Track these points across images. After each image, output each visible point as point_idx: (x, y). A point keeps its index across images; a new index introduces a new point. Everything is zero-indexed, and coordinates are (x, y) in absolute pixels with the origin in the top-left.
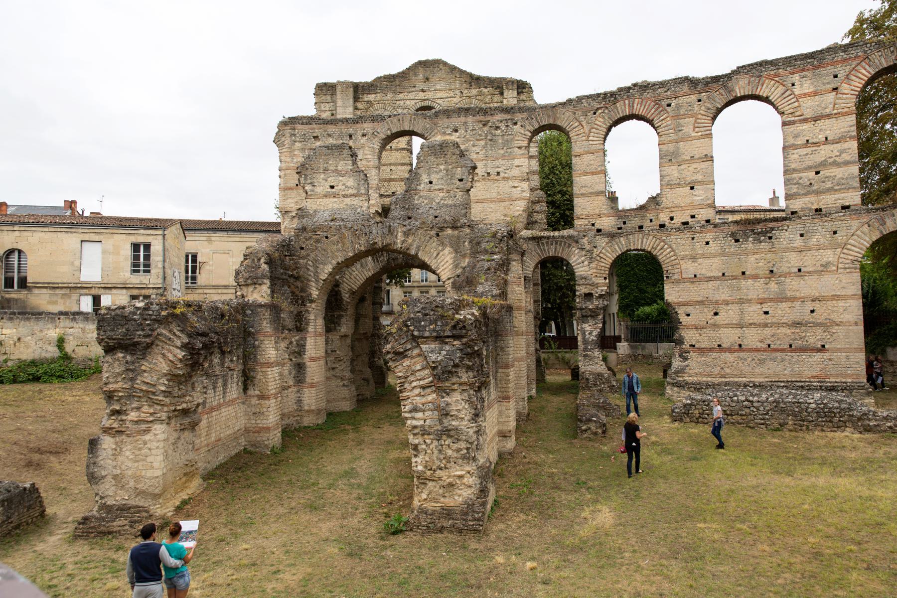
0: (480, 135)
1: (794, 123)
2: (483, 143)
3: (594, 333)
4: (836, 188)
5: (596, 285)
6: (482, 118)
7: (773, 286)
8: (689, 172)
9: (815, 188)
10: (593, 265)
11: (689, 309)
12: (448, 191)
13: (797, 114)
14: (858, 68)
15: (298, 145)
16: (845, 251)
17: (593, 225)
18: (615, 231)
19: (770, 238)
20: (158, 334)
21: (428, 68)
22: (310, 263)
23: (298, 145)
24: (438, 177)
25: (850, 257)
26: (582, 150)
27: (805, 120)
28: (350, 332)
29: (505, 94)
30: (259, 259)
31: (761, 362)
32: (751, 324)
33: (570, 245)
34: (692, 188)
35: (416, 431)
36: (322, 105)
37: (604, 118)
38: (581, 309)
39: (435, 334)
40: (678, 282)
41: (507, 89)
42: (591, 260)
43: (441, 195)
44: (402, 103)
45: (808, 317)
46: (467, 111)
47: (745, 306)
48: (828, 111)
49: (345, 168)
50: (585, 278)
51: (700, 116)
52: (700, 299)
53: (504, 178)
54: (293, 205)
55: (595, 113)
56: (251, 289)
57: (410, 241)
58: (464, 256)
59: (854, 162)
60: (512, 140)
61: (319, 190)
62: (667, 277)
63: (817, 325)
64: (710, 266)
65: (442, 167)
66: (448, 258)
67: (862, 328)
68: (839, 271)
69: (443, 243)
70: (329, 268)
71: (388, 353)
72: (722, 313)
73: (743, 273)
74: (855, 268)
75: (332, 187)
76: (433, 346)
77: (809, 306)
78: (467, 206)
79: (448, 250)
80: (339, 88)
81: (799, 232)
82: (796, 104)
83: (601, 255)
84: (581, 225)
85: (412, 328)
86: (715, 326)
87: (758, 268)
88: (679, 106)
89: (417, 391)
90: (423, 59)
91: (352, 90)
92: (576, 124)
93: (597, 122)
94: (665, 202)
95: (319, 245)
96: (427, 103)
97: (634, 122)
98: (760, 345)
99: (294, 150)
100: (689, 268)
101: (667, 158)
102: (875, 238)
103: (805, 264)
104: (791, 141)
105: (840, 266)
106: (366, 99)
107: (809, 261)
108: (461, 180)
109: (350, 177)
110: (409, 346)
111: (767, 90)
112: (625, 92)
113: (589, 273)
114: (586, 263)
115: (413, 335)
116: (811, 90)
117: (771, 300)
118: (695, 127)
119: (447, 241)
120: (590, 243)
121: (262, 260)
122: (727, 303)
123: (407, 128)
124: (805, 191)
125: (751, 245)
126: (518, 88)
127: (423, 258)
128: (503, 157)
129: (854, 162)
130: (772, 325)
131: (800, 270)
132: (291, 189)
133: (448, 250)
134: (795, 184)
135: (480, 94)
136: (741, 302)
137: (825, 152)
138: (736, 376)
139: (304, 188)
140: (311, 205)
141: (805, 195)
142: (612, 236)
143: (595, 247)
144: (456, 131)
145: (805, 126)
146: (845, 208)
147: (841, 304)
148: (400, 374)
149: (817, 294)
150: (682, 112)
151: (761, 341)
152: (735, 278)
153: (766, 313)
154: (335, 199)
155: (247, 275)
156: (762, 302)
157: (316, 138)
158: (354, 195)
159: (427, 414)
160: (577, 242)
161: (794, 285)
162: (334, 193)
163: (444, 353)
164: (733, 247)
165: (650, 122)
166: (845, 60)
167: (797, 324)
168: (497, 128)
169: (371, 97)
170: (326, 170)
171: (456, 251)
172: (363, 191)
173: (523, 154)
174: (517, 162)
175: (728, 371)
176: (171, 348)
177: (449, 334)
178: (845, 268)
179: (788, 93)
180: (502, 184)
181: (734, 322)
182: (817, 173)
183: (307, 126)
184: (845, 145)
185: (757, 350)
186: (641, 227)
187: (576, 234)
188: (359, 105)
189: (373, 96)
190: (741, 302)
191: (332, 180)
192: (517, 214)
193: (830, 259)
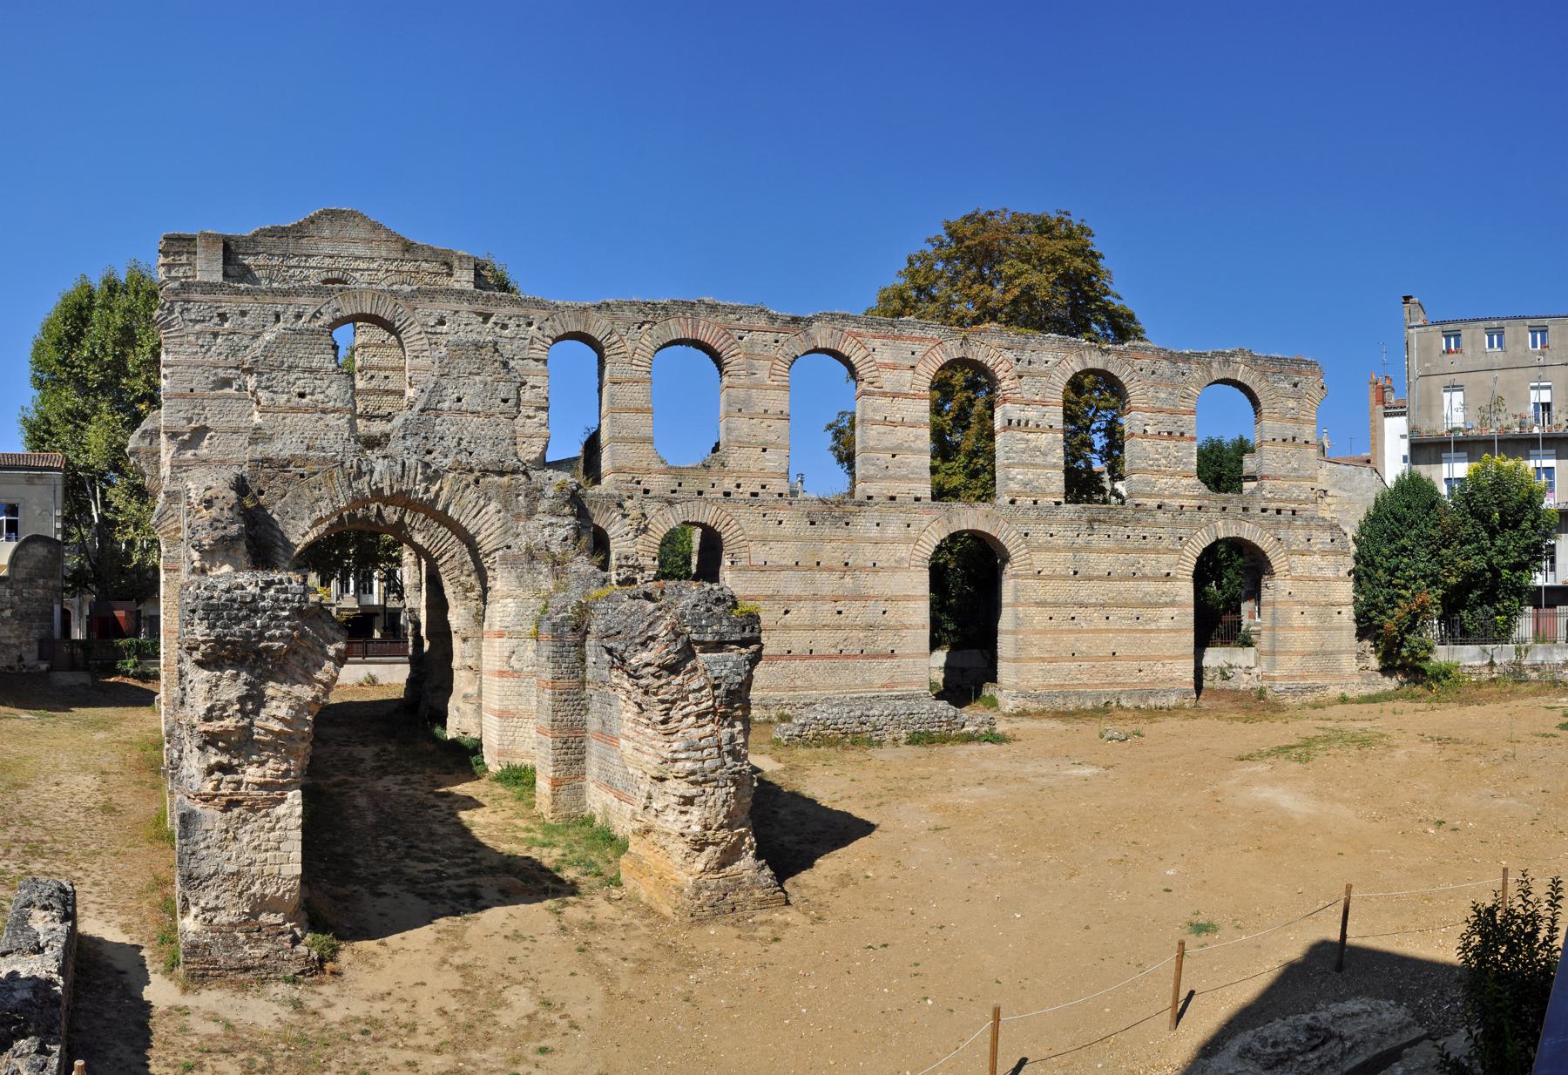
1: (871, 394)
27: (885, 394)
31: (833, 670)
35: (692, 778)
45: (881, 619)
48: (906, 389)
63: (888, 628)
71: (647, 665)
72: (793, 612)
77: (882, 606)
86: (786, 628)
89: (692, 719)
94: (731, 463)
98: (833, 651)
100: (759, 554)
107: (884, 556)
117: (846, 598)
122: (799, 599)
130: (846, 626)
138: (806, 688)
146: (917, 499)
147: (912, 604)
148: (667, 697)
151: (835, 646)
153: (840, 612)
159: (706, 752)
160: (620, 505)
163: (730, 664)
164: (810, 531)
167: (870, 627)
175: (798, 683)
184: (920, 431)
185: (830, 657)
190: (815, 598)
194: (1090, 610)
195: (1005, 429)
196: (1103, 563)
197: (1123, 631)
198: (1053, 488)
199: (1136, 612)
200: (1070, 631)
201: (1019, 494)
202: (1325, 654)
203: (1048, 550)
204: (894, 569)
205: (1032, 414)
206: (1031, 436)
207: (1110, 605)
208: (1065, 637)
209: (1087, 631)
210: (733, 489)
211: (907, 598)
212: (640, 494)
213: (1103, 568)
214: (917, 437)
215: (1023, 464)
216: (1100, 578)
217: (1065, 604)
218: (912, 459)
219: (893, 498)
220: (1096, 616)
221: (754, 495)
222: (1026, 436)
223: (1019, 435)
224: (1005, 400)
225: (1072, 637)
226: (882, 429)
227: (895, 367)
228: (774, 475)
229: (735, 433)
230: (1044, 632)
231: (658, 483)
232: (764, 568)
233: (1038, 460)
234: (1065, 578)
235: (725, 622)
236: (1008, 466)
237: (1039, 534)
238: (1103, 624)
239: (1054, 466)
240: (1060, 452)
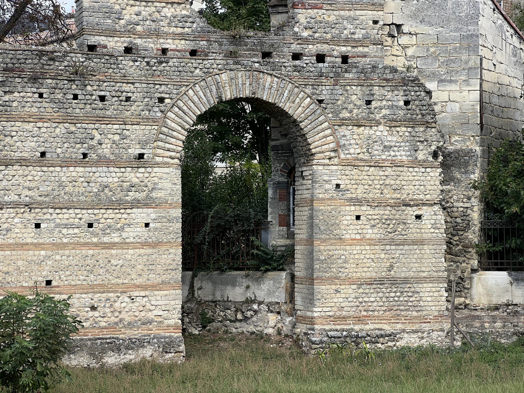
197: (64, 246)
199: (87, 216)
202: (394, 282)
207: (41, 206)
213: (29, 148)
216: (23, 162)
238: (29, 235)
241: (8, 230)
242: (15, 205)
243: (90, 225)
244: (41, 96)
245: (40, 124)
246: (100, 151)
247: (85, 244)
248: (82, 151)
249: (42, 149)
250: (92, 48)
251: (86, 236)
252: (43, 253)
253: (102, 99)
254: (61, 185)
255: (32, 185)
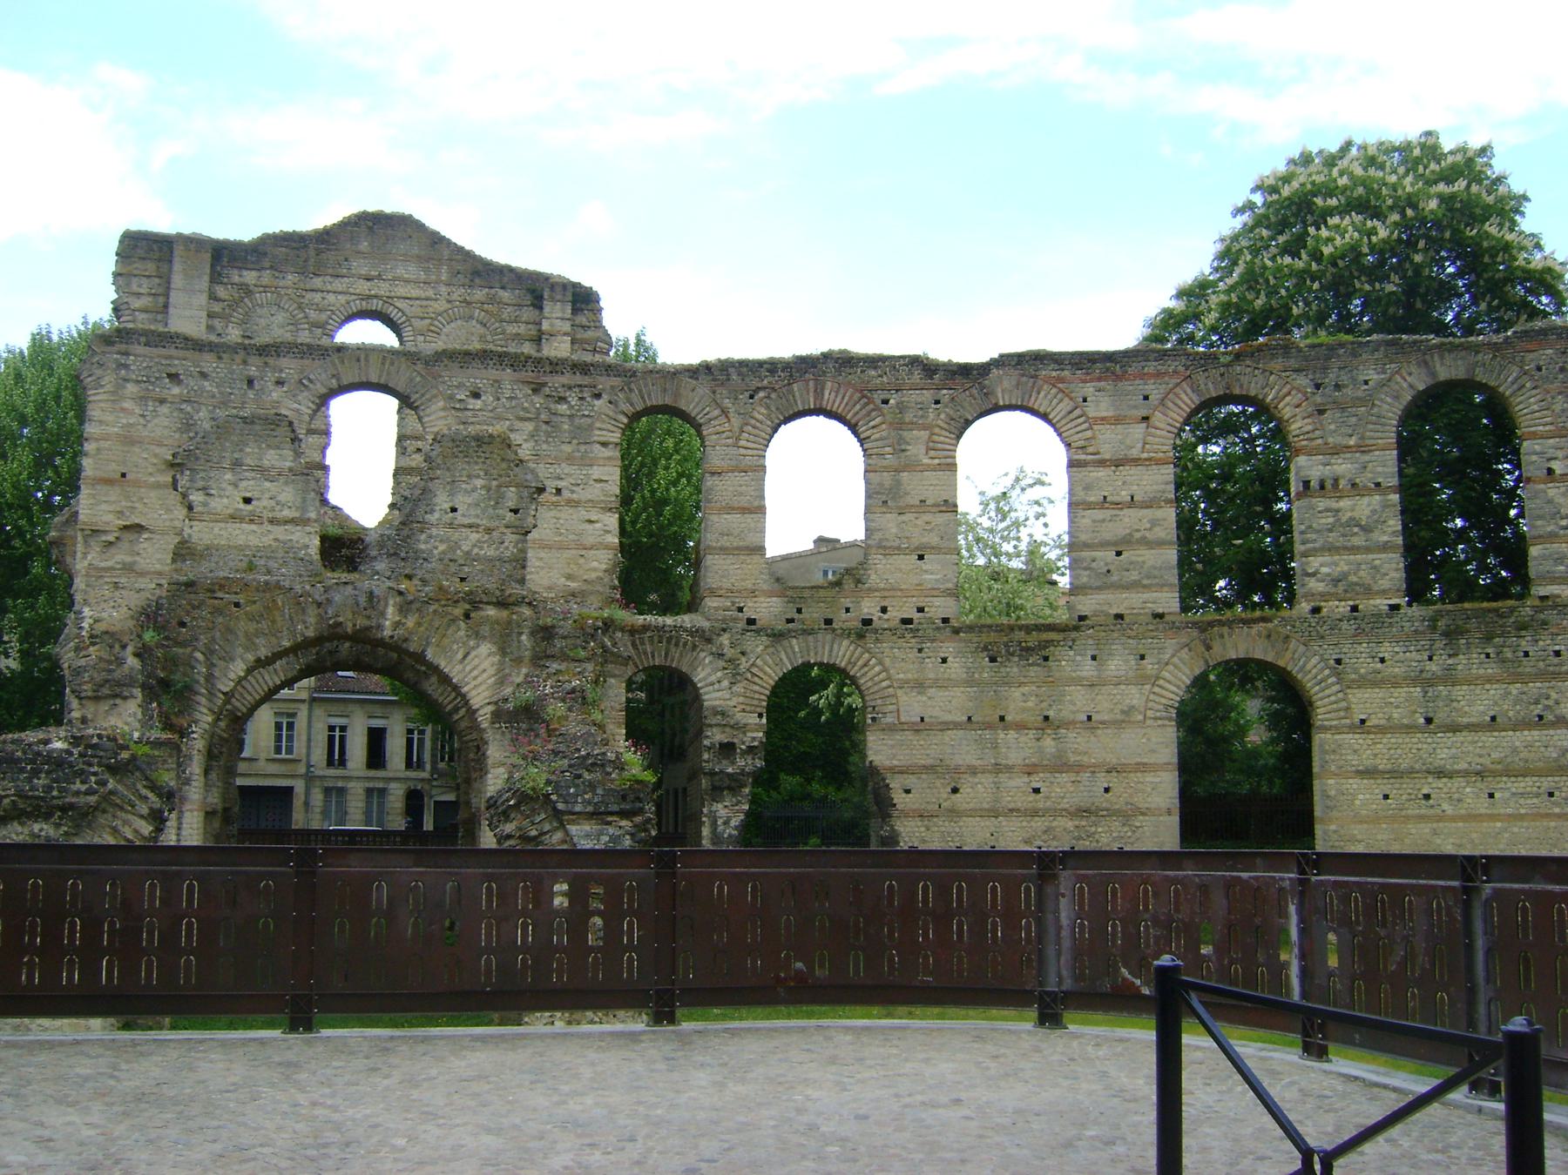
0: (524, 409)
2: (530, 426)
3: (734, 822)
4: (1145, 582)
5: (743, 728)
6: (528, 375)
7: (1048, 743)
8: (917, 529)
9: (1115, 578)
10: (738, 688)
11: (910, 781)
12: (489, 531)
13: (1091, 450)
14: (1178, 390)
15: (131, 388)
16: (1156, 689)
17: (740, 610)
18: (781, 626)
19: (1046, 659)
20: (111, 793)
21: (380, 231)
22: (199, 655)
23: (131, 388)
24: (469, 500)
25: (1164, 701)
26: (725, 464)
27: (1102, 463)
28: (219, 807)
29: (547, 309)
30: (124, 647)
32: (1011, 810)
33: (694, 647)
34: (921, 557)
36: (135, 280)
37: (768, 407)
38: (712, 774)
39: (590, 809)
40: (891, 729)
41: (552, 299)
42: (736, 677)
43: (474, 536)
44: (317, 297)
45: (1102, 800)
46: (502, 359)
47: (1003, 777)
48: (1134, 453)
49: (277, 464)
50: (723, 714)
51: (937, 430)
52: (929, 762)
53: (569, 502)
54: (110, 517)
55: (752, 397)
56: (104, 706)
57: (410, 622)
58: (518, 661)
59: (1170, 543)
60: (591, 427)
61: (217, 504)
62: (873, 719)
64: (948, 703)
65: (479, 483)
66: (486, 664)
67: (1177, 818)
68: (1149, 722)
69: (477, 634)
70: (238, 668)
73: (1002, 718)
74: (1170, 719)
75: (247, 501)
76: (587, 828)
77: (1102, 780)
78: (521, 562)
79: (485, 648)
80: (178, 251)
81: (1090, 653)
82: (1089, 434)
83: (754, 670)
84: (716, 609)
85: (554, 797)
86: (954, 813)
87: (1024, 710)
88: (901, 407)
90: (372, 208)
91: (208, 256)
92: (717, 412)
93: (760, 417)
94: (873, 579)
95: (220, 619)
96: (376, 305)
97: (821, 420)
99: (123, 398)
100: (912, 706)
101: (879, 498)
102: (1197, 672)
103: (1099, 708)
104: (1081, 495)
105: (1150, 713)
106: (236, 279)
107: (1104, 705)
108: (515, 511)
109: (286, 483)
110: (547, 827)
111: (1046, 403)
112: (804, 367)
113: (732, 703)
114: (725, 683)
115: (555, 809)
116: (1110, 414)
118: (928, 449)
119: (485, 630)
120: (733, 645)
121: (130, 649)
122: (974, 771)
123: (374, 379)
124: (1098, 584)
125: (1015, 669)
126: (574, 303)
127: (436, 661)
128: (570, 459)
129: (1170, 543)
130: (1045, 812)
131: (1089, 718)
132: (109, 482)
133: (485, 648)
134: (1085, 569)
135: (492, 300)
136: (998, 769)
137: (1131, 520)
139: (184, 496)
140: (200, 533)
141: (1099, 588)
142: (777, 636)
143: (743, 653)
144: (476, 395)
145: (1102, 473)
147: (1149, 778)
149: (1114, 761)
150: (909, 417)
152: (989, 726)
153: (1036, 791)
154: (254, 527)
155: (99, 678)
156: (1030, 771)
157: (174, 377)
158: (292, 521)
161: (1077, 743)
162: (252, 513)
164: (986, 672)
165: (853, 429)
166: (1158, 375)
167: (1083, 812)
168: (562, 399)
169: (250, 277)
170: (237, 464)
171: (503, 651)
172: (313, 515)
173: (609, 458)
174: (596, 472)
176: (130, 816)
177: (615, 808)
178: (1156, 719)
179: (1077, 412)
180: (566, 513)
181: (986, 806)
182: (1119, 554)
183: (155, 350)
184: (1159, 513)
186: (828, 622)
187: (706, 624)
188: (221, 291)
189: (254, 274)
190: (998, 769)
191: (249, 487)
192: (594, 575)
193: (1135, 702)
194: (1458, 782)
195: (1299, 496)
196: (1476, 702)
197: (1522, 817)
198: (1384, 583)
199: (1547, 783)
200: (1421, 818)
201: (1325, 596)
203: (1375, 684)
204: (1118, 724)
205: (1343, 467)
206: (1344, 503)
207: (1495, 774)
208: (1412, 828)
209: (1453, 819)
210: (876, 616)
211: (1142, 768)
212: (742, 625)
214: (1154, 523)
215: (1331, 549)
216: (1472, 728)
217: (1411, 772)
218: (1149, 557)
219: (1119, 617)
220: (1471, 795)
221: (907, 621)
222: (1333, 504)
223: (1321, 504)
224: (1298, 452)
225: (1426, 828)
226: (1098, 514)
227: (1118, 420)
228: (934, 592)
229: (877, 536)
230: (1375, 819)
231: (767, 609)
232: (922, 725)
233: (1358, 541)
234: (1409, 729)
235: (599, 791)
236: (1305, 555)
237: (1360, 659)
238: (1483, 806)
239: (1385, 548)
240: (1395, 524)
241: (1459, 800)
242: (1466, 774)
243: (1551, 795)
244: (1488, 656)
245: (1488, 686)
246: (1558, 712)
247: (1548, 815)
248: (1537, 712)
249: (1492, 713)
250: (1543, 598)
251: (1542, 804)
252: (1499, 824)
253: (1558, 654)
254: (1515, 750)
255: (1484, 752)
